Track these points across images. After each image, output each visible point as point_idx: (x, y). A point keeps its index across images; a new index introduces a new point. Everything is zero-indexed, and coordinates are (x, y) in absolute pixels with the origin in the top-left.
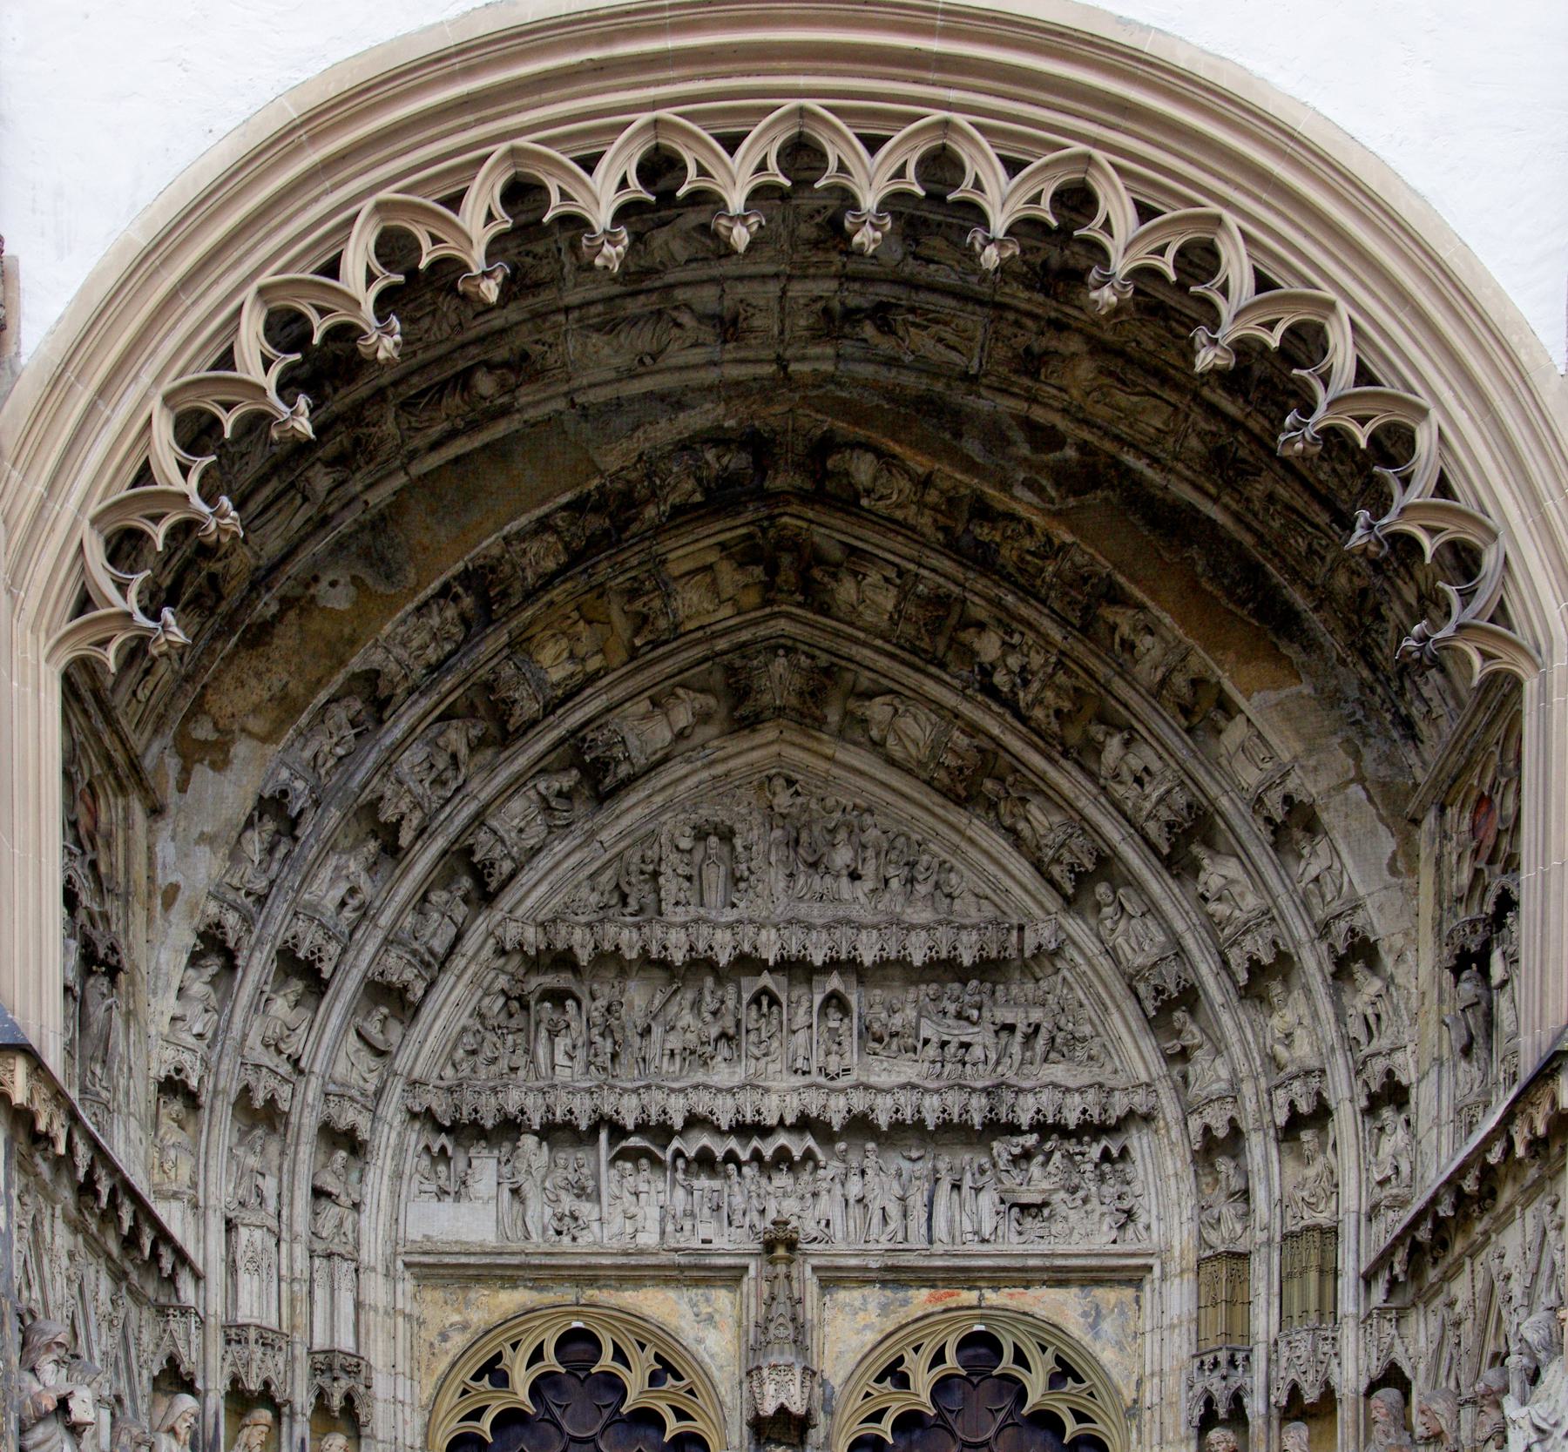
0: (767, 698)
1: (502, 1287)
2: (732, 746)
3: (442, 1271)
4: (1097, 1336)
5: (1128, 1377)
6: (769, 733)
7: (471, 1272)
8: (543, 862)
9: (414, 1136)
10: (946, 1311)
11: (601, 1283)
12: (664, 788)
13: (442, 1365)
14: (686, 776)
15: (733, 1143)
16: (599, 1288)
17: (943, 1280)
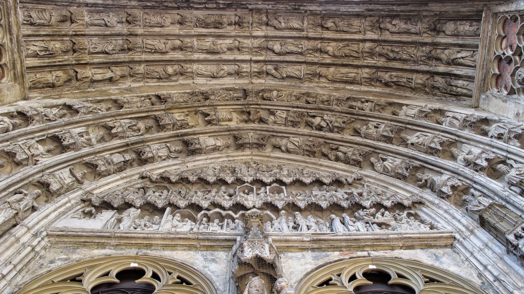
0: (247, 141)
1: (98, 248)
2: (235, 154)
3: (66, 240)
4: (441, 263)
5: (471, 274)
6: (248, 152)
7: (83, 240)
8: (165, 163)
9: (79, 207)
10: (350, 258)
11: (153, 248)
12: (211, 159)
13: (44, 271)
14: (219, 158)
15: (231, 212)
16: (151, 250)
17: (346, 247)
